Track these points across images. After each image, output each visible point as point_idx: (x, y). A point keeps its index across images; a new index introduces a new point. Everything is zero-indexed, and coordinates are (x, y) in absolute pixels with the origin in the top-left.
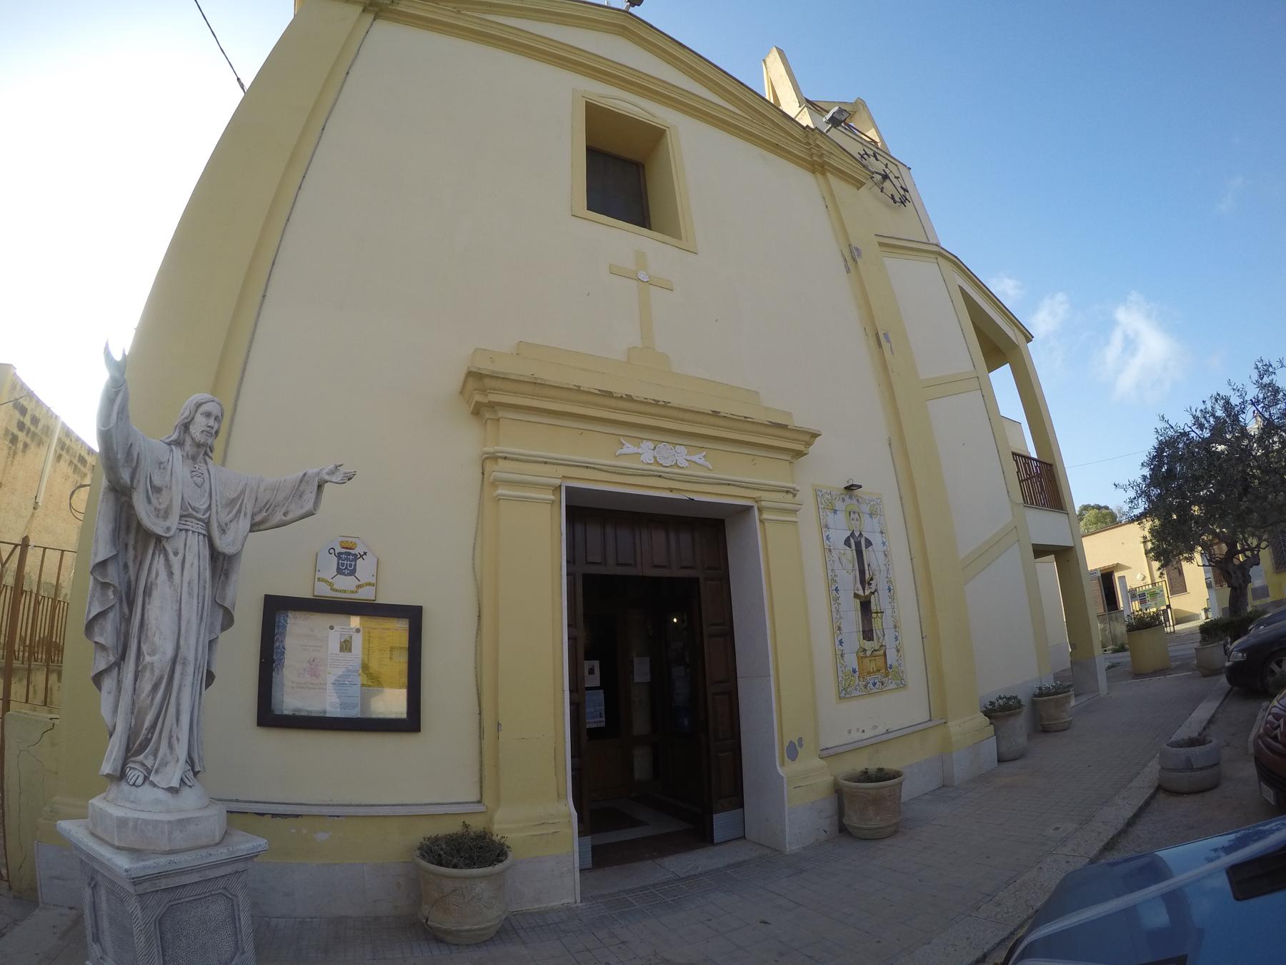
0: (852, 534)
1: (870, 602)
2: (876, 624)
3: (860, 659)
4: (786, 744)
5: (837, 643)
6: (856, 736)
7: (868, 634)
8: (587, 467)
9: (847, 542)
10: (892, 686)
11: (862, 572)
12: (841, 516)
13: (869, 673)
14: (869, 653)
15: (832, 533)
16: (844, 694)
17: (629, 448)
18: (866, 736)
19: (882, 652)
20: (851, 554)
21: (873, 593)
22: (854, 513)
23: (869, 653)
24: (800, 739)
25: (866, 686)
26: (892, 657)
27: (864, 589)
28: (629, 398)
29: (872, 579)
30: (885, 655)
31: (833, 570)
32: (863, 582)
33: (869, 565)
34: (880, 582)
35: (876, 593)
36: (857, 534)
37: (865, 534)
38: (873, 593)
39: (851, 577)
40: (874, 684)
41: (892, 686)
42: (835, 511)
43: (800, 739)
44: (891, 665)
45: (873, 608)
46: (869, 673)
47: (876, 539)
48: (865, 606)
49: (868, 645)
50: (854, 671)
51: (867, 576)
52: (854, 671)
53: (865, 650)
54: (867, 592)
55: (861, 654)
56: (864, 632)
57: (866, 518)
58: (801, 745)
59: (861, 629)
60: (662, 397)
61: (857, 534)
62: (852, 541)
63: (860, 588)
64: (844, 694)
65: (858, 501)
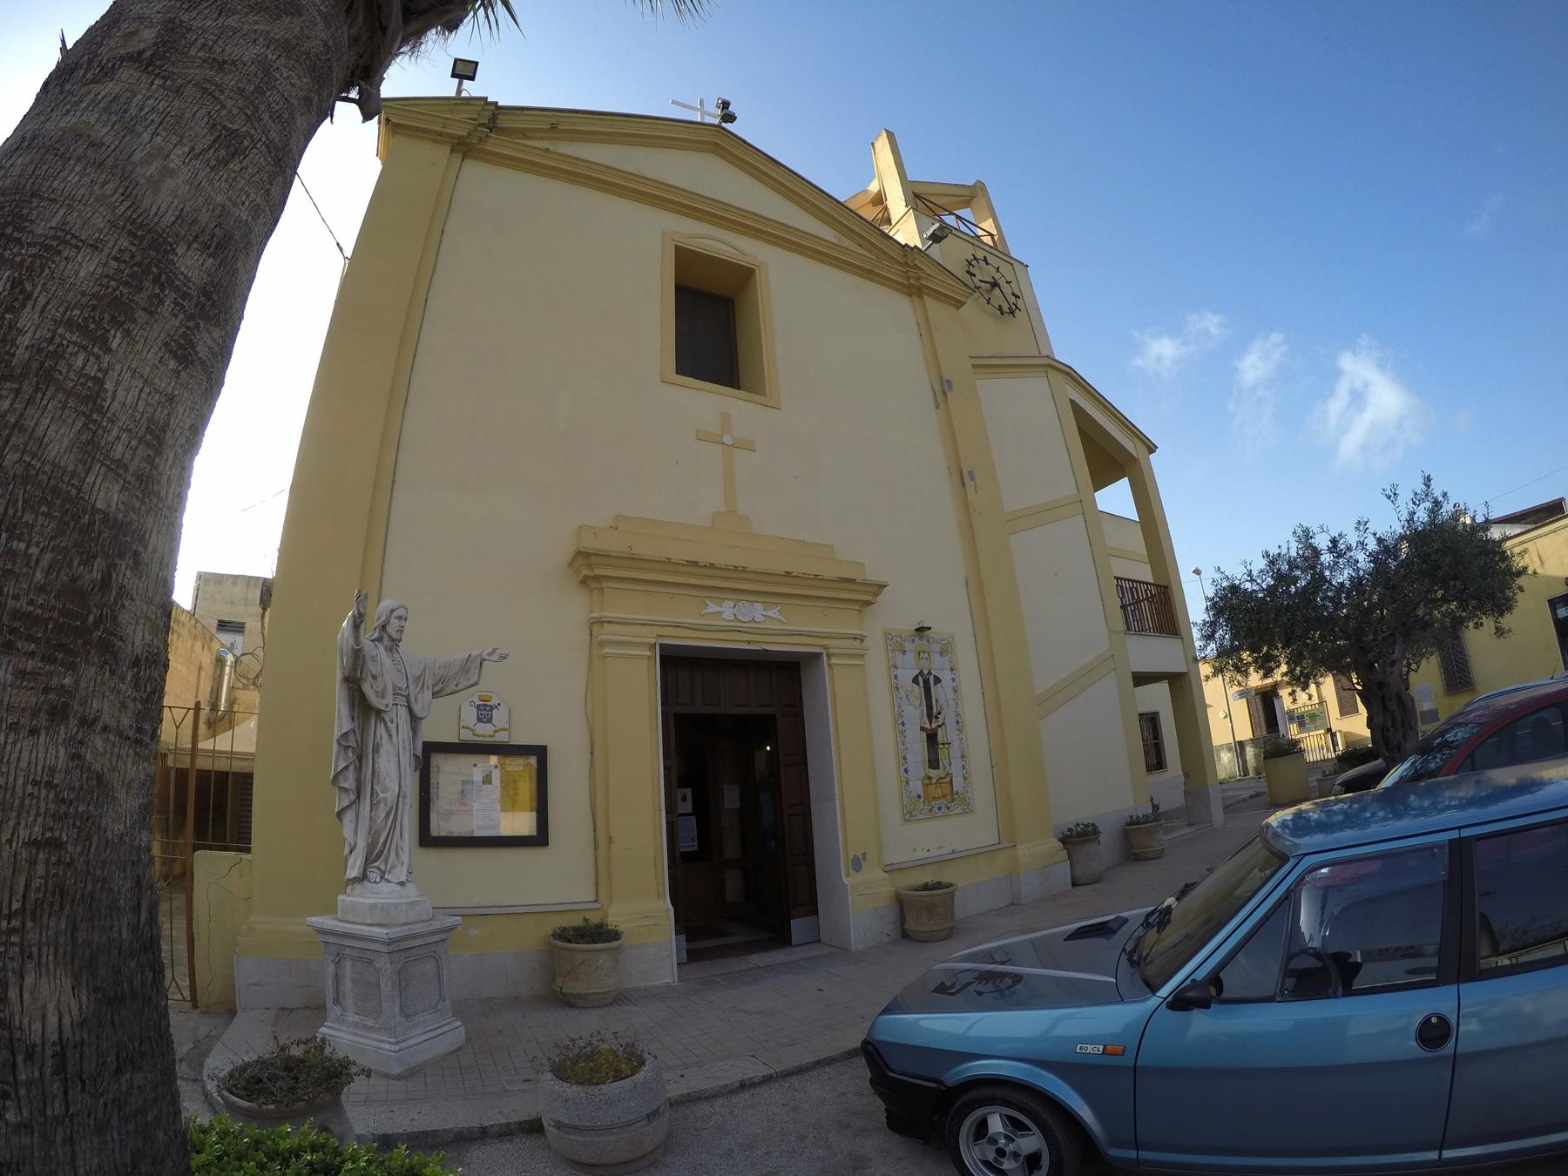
0: (921, 673)
1: (936, 735)
2: (942, 753)
3: (925, 786)
4: (851, 857)
5: (902, 771)
6: (920, 854)
7: (934, 763)
9: (915, 680)
10: (959, 811)
11: (930, 707)
12: (910, 657)
13: (934, 798)
14: (934, 781)
15: (900, 672)
16: (909, 816)
17: (713, 608)
18: (930, 855)
19: (948, 780)
20: (919, 691)
21: (940, 726)
22: (924, 652)
23: (934, 781)
24: (864, 854)
25: (931, 811)
26: (958, 784)
27: (931, 723)
28: (712, 566)
29: (939, 713)
30: (951, 782)
31: (899, 706)
32: (930, 716)
33: (937, 701)
34: (948, 717)
35: (943, 726)
36: (926, 672)
37: (933, 672)
38: (940, 726)
39: (918, 711)
40: (940, 809)
41: (959, 811)
42: (904, 652)
43: (864, 854)
44: (957, 792)
45: (940, 739)
46: (934, 798)
47: (945, 676)
48: (932, 738)
49: (934, 773)
50: (919, 797)
51: (935, 711)
52: (919, 797)
53: (930, 778)
54: (934, 726)
55: (927, 782)
56: (929, 761)
57: (936, 658)
58: (865, 859)
59: (927, 759)
60: (740, 563)
61: (926, 672)
62: (920, 678)
63: (927, 721)
64: (909, 816)
65: (928, 641)
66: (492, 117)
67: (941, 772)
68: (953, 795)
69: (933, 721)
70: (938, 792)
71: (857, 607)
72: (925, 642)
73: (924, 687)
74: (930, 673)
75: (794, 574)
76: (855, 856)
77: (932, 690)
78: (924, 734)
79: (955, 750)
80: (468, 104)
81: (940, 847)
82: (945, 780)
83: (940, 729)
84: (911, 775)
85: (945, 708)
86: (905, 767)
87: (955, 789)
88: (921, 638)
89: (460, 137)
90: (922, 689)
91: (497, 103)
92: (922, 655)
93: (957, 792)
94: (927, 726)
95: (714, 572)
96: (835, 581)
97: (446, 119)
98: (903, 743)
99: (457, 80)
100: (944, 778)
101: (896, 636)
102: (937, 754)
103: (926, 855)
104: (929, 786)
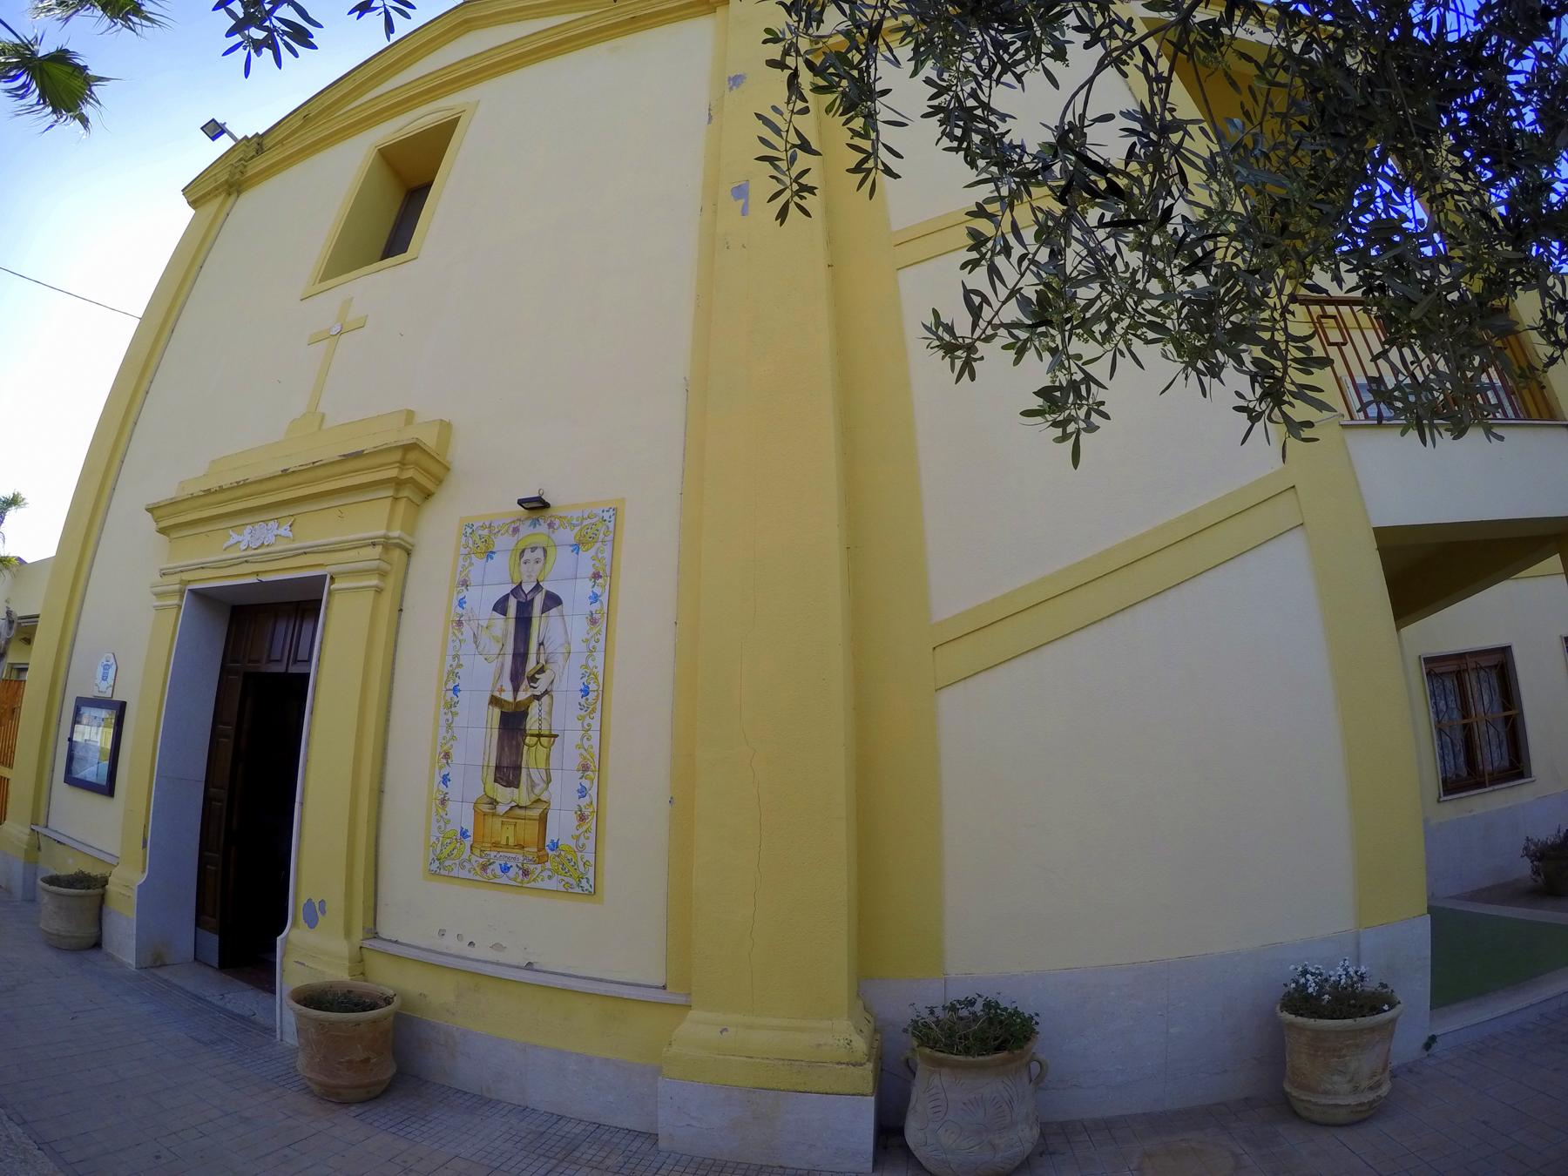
0: (516, 592)
1: (525, 714)
2: (532, 758)
3: (480, 816)
4: (303, 900)
5: (438, 779)
6: (451, 944)
7: (508, 773)
8: (202, 568)
9: (501, 607)
10: (552, 884)
11: (520, 657)
12: (501, 562)
13: (496, 845)
14: (502, 809)
15: (472, 595)
16: (439, 868)
17: (235, 538)
18: (474, 953)
19: (536, 813)
20: (505, 626)
21: (538, 698)
22: (533, 549)
23: (502, 809)
24: (322, 902)
25: (484, 868)
26: (561, 826)
27: (516, 690)
28: (221, 490)
29: (542, 670)
30: (543, 820)
31: (456, 657)
32: (516, 678)
33: (541, 644)
34: (564, 679)
35: (545, 699)
36: (527, 588)
37: (546, 586)
38: (538, 698)
39: (492, 668)
40: (505, 869)
41: (552, 884)
42: (490, 554)
43: (322, 902)
44: (555, 846)
45: (532, 724)
46: (496, 845)
47: (576, 593)
48: (512, 722)
49: (504, 795)
50: (464, 834)
51: (531, 665)
52: (464, 834)
53: (493, 803)
54: (522, 696)
55: (486, 808)
56: (498, 768)
57: (561, 559)
58: (323, 912)
59: (493, 763)
61: (527, 588)
62: (513, 603)
63: (508, 686)
64: (439, 868)
65: (550, 525)
66: (258, 144)
67: (521, 795)
68: (543, 849)
69: (523, 687)
70: (508, 834)
71: (390, 493)
72: (543, 528)
73: (517, 619)
74: (538, 587)
75: (291, 470)
76: (310, 900)
77: (535, 623)
78: (497, 712)
79: (568, 753)
80: (234, 151)
81: (497, 947)
82: (529, 813)
83: (536, 703)
84: (454, 789)
85: (560, 659)
86: (444, 772)
87: (551, 836)
88: (535, 522)
89: (227, 181)
90: (512, 623)
91: (257, 134)
92: (528, 555)
93: (555, 846)
94: (508, 696)
95: (248, 490)
96: (338, 461)
97: (215, 175)
98: (449, 726)
99: (240, 137)
100: (525, 808)
101: (483, 527)
102: (519, 754)
103: (460, 948)
104: (489, 820)
